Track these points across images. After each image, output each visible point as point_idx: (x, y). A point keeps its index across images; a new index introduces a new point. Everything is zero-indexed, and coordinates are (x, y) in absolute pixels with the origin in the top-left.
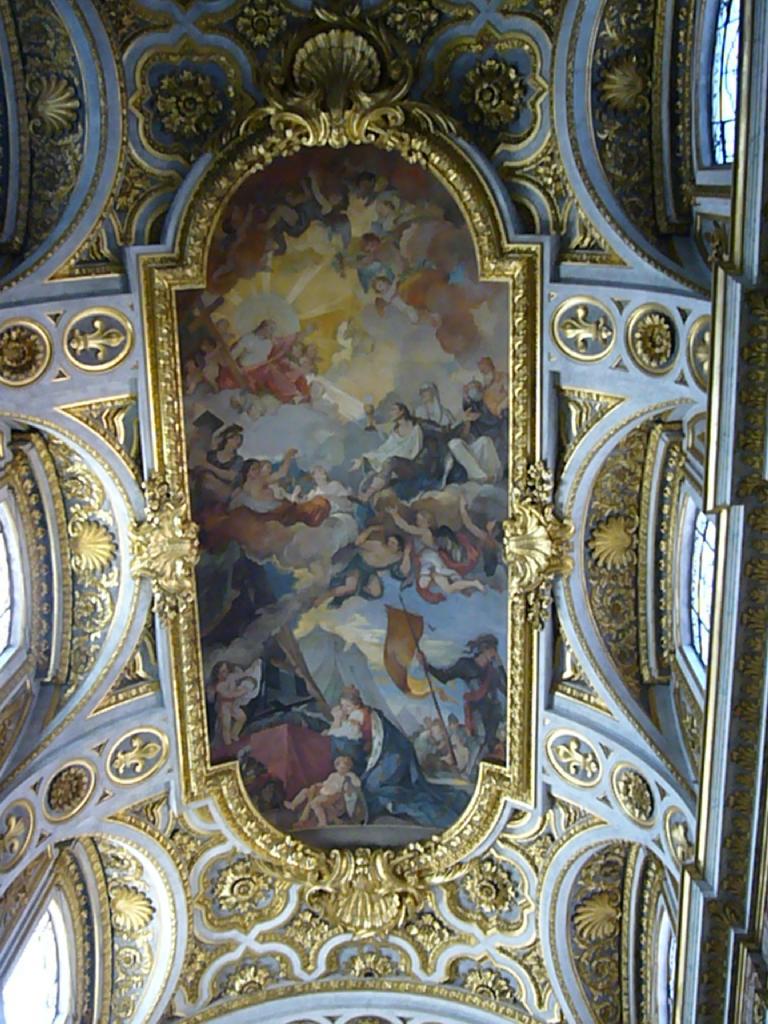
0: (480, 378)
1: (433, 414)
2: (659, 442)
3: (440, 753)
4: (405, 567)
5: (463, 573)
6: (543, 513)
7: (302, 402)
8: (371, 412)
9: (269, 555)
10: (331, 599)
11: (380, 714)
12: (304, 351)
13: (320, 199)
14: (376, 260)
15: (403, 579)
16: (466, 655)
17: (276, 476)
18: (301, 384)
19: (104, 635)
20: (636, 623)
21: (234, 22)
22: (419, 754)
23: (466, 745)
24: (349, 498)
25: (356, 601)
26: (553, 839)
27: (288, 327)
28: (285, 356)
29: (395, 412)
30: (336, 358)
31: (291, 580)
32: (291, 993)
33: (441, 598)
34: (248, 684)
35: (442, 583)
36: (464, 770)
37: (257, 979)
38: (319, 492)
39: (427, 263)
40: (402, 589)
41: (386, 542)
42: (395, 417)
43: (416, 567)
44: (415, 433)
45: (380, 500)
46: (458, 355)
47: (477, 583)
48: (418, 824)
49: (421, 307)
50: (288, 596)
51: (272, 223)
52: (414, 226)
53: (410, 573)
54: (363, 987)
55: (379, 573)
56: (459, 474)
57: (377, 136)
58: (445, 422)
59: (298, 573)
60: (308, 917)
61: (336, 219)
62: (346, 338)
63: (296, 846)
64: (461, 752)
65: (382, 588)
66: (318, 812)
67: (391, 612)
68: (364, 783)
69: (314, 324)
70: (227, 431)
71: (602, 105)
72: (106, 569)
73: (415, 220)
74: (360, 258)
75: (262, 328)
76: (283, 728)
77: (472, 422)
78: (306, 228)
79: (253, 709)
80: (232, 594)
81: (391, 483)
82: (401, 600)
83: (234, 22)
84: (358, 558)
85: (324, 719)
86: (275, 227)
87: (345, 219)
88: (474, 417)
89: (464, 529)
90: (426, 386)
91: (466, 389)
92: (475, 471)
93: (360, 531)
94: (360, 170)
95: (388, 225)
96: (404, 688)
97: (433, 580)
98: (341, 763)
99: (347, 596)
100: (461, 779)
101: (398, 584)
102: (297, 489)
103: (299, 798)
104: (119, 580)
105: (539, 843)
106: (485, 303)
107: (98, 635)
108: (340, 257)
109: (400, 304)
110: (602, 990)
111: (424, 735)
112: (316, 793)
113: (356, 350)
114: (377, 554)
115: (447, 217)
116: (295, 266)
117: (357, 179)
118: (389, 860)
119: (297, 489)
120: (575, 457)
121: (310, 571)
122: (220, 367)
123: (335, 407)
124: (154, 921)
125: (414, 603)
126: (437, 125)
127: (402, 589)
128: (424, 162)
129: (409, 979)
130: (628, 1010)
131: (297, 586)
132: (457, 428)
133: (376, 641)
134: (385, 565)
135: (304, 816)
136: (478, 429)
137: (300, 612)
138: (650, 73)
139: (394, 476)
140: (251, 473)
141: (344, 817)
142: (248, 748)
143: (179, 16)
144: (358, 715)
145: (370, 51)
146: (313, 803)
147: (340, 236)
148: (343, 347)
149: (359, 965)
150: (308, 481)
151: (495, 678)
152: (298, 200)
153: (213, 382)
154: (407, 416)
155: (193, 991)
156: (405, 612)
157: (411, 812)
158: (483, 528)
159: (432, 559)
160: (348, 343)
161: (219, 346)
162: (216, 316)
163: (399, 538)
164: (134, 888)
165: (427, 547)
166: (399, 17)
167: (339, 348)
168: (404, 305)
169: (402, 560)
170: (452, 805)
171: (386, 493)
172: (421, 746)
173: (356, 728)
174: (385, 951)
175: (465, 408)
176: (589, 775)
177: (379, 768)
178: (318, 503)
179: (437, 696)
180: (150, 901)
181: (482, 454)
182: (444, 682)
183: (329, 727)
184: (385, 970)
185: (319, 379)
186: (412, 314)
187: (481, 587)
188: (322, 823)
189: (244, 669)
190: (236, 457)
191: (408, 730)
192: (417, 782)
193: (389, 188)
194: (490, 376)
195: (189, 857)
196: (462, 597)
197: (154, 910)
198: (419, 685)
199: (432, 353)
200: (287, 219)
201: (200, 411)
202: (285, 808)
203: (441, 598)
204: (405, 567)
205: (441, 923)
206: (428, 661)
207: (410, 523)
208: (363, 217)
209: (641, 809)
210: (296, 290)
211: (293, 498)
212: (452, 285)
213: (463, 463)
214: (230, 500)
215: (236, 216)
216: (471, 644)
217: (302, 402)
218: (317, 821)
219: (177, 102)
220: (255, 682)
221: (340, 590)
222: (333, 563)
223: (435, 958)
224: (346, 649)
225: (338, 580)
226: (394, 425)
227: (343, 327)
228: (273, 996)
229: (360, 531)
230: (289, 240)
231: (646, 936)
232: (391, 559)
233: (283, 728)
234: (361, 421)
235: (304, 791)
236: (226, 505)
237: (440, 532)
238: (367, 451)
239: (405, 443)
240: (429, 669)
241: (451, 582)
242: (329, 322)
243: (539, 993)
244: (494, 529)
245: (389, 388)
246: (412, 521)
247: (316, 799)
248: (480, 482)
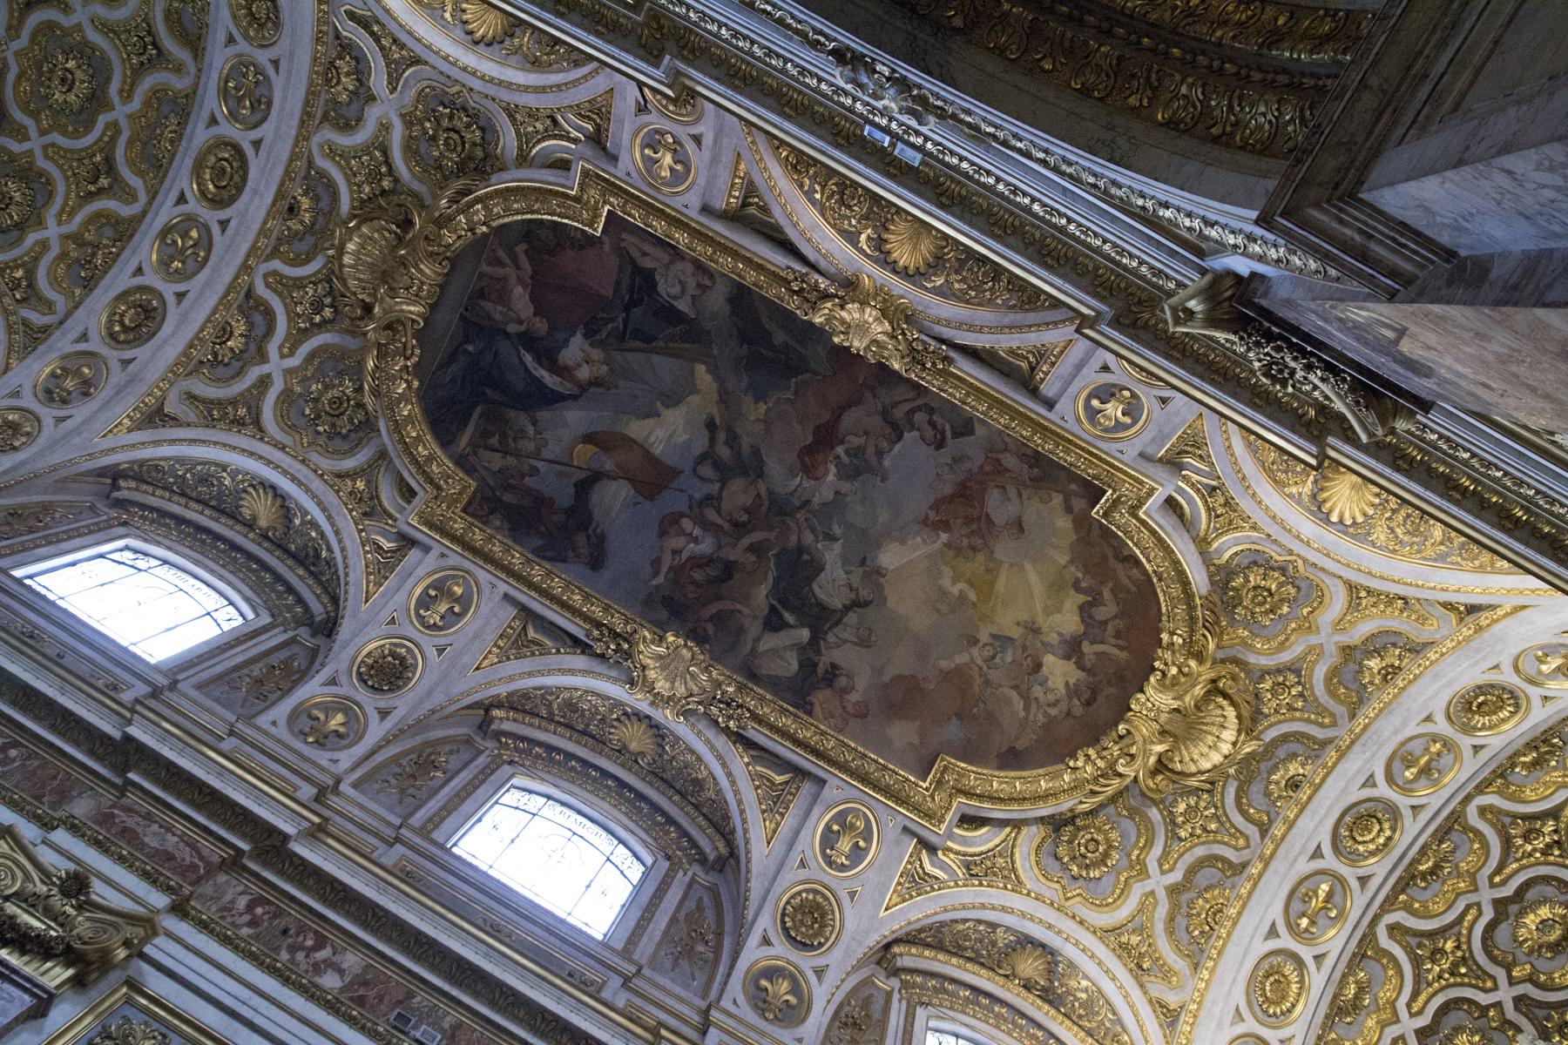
0: (854, 697)
1: (845, 630)
2: (710, 846)
3: (504, 436)
4: (711, 514)
5: (677, 571)
6: (699, 703)
7: (927, 517)
8: (880, 572)
9: (796, 393)
10: (718, 422)
11: (574, 397)
12: (973, 549)
13: (1100, 648)
14: (1013, 661)
15: (701, 504)
16: (594, 524)
17: (871, 450)
18: (945, 525)
19: (813, 202)
20: (551, 719)
21: (1298, 673)
22: (512, 414)
23: (501, 471)
24: (807, 502)
25: (701, 444)
26: (365, 514)
27: (1004, 549)
28: (980, 529)
29: (865, 594)
30: (947, 572)
31: (760, 397)
32: (307, 115)
33: (663, 533)
34: (676, 290)
35: (677, 542)
36: (475, 453)
37: (340, 88)
38: (831, 477)
39: (982, 706)
40: (691, 497)
41: (746, 510)
42: (861, 591)
43: (706, 525)
44: (836, 603)
45: (789, 528)
46: (886, 686)
47: (660, 580)
48: (441, 367)
49: (946, 676)
50: (744, 384)
51: (1107, 594)
52: (1022, 714)
53: (702, 514)
54: (280, 195)
55: (717, 485)
56: (773, 623)
57: (1121, 737)
58: (831, 638)
59: (763, 408)
60: (386, 184)
61: (1072, 649)
62: (962, 594)
63: (474, 234)
64: (496, 461)
65: (701, 478)
66: (502, 271)
67: (675, 473)
68: (508, 336)
69: (992, 571)
70: (943, 438)
71: (1026, 942)
72: (879, 243)
73: (1026, 718)
74: (1025, 648)
75: (1019, 526)
76: (609, 293)
77: (816, 665)
78: (1081, 617)
79: (644, 281)
80: (780, 337)
81: (800, 549)
82: (681, 491)
83: (1298, 673)
84: (745, 474)
85: (597, 337)
86: (1100, 594)
87: (1068, 658)
88: (820, 670)
89: (718, 598)
90: (873, 639)
91: (850, 676)
92: (770, 642)
93: (770, 492)
94: (1101, 699)
95: (1037, 691)
96: (589, 438)
97: (685, 535)
98: (541, 326)
99: (712, 439)
100: (468, 444)
101: (698, 496)
102: (846, 460)
103: (524, 261)
104: (861, 251)
105: (366, 496)
106: (916, 740)
107: (818, 196)
108: (1037, 631)
109: (961, 659)
110: (183, 477)
111: (531, 430)
112: (520, 281)
113: (943, 592)
114: (738, 495)
115: (1012, 750)
116: (1056, 588)
117: (1095, 691)
118: (413, 321)
119: (846, 460)
120: (739, 761)
121: (758, 420)
122: (1007, 470)
123: (903, 542)
124: (463, 34)
125: (672, 501)
126: (1093, 793)
127: (691, 497)
128: (1071, 764)
129: (268, 251)
130: (153, 495)
131: (748, 400)
132: (818, 645)
133: (653, 439)
134: (724, 495)
135: (501, 253)
136: (808, 666)
137: (721, 384)
138: (1025, 987)
139: (806, 557)
140: (889, 430)
141: (481, 294)
142: (607, 248)
143: (1337, 638)
144: (584, 373)
145: (1193, 769)
146: (510, 271)
147: (1055, 643)
148: (953, 583)
149: (305, 203)
150: (846, 474)
151: (554, 549)
152: (1110, 627)
153: (1000, 456)
154: (857, 604)
155: (352, 16)
156: (666, 487)
157: (454, 367)
158: (711, 619)
159: (706, 547)
160: (955, 590)
161: (1029, 483)
162: (1057, 499)
163: (744, 525)
164: (512, 36)
165: (720, 547)
166: (1203, 804)
167: (955, 581)
168: (958, 661)
169: (718, 512)
170: (444, 420)
171: (793, 539)
172: (521, 419)
173: (571, 363)
174: (310, 240)
175: (834, 666)
176: (422, 612)
177: (517, 362)
178: (821, 470)
179: (563, 468)
180: (489, 45)
181: (782, 658)
182: (575, 485)
183: (586, 336)
184: (289, 229)
185: (938, 545)
186: (945, 664)
187: (655, 582)
188: (485, 268)
189: (693, 297)
190: (913, 428)
191: (544, 415)
192: (484, 394)
193: (1069, 714)
194: (849, 708)
195: (518, 117)
196: (654, 557)
197: (476, 43)
198: (584, 454)
199: (900, 662)
200: (1102, 609)
201: (980, 431)
202: (520, 242)
203: (663, 533)
204: (711, 514)
205: (319, 326)
206: (606, 481)
207: (751, 544)
208: (1059, 673)
209: (372, 667)
210: (1033, 576)
211: (840, 450)
212: (949, 719)
213: (782, 634)
214: (874, 396)
215: (1135, 572)
216: (602, 538)
217: (927, 517)
218: (489, 264)
219: (1269, 590)
220: (675, 298)
221: (722, 436)
222: (752, 447)
223: (280, 295)
224: (658, 404)
225: (733, 440)
226: (855, 586)
227: (972, 596)
228: (311, 93)
229: (770, 492)
230: (1081, 598)
231: (223, 551)
232: (727, 505)
233: (609, 293)
234: (876, 557)
235: (530, 272)
236: (873, 389)
237: (729, 569)
238: (844, 546)
239: (832, 585)
240: (596, 477)
241: (675, 552)
242: (986, 588)
243: (204, 401)
244: (705, 630)
245: (891, 604)
246: (754, 549)
247: (514, 276)
248: (757, 640)
